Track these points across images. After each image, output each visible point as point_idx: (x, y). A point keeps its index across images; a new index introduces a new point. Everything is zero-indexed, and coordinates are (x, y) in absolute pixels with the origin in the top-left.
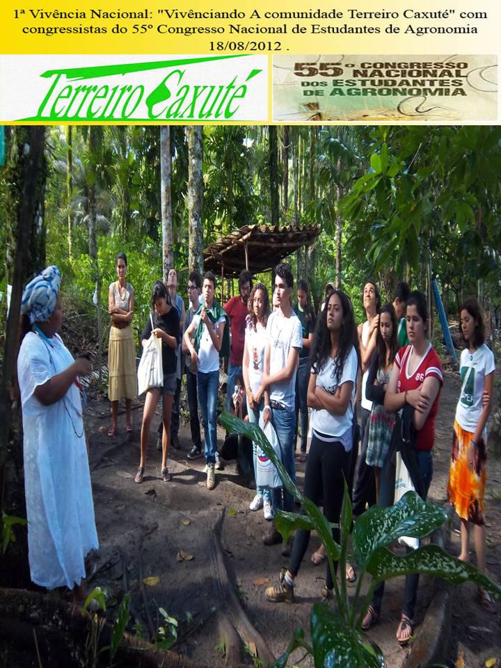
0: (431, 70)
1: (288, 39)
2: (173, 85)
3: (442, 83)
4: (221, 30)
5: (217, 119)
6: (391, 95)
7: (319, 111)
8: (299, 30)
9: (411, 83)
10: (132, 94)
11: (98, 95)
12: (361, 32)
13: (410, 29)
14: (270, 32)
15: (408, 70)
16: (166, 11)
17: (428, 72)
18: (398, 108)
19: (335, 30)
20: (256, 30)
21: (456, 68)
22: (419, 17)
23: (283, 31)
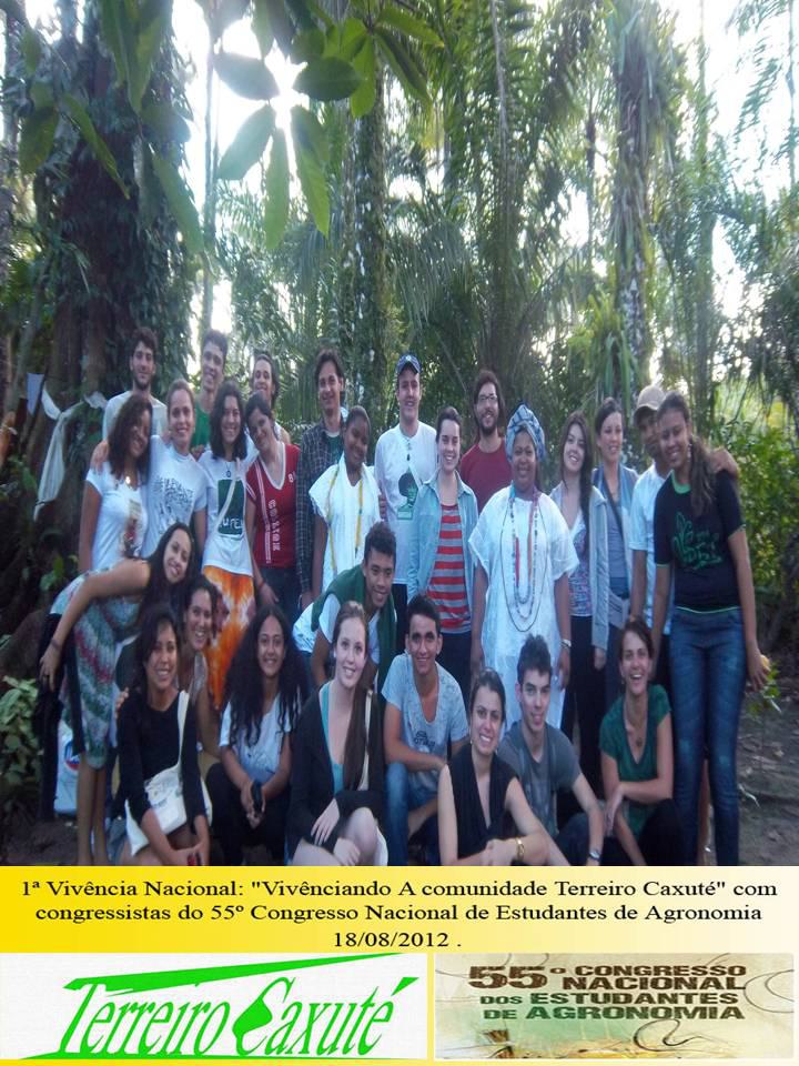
0: (687, 979)
1: (459, 929)
2: (275, 1002)
3: (705, 998)
4: (352, 914)
5: (346, 1056)
6: (624, 1018)
7: (509, 1043)
8: (476, 914)
9: (656, 999)
10: (211, 1016)
11: (157, 1018)
12: (576, 918)
13: (653, 912)
14: (430, 918)
15: (650, 978)
16: (266, 883)
17: (682, 980)
18: (635, 1039)
19: (535, 915)
20: (408, 914)
21: (728, 975)
22: (668, 894)
23: (451, 915)
